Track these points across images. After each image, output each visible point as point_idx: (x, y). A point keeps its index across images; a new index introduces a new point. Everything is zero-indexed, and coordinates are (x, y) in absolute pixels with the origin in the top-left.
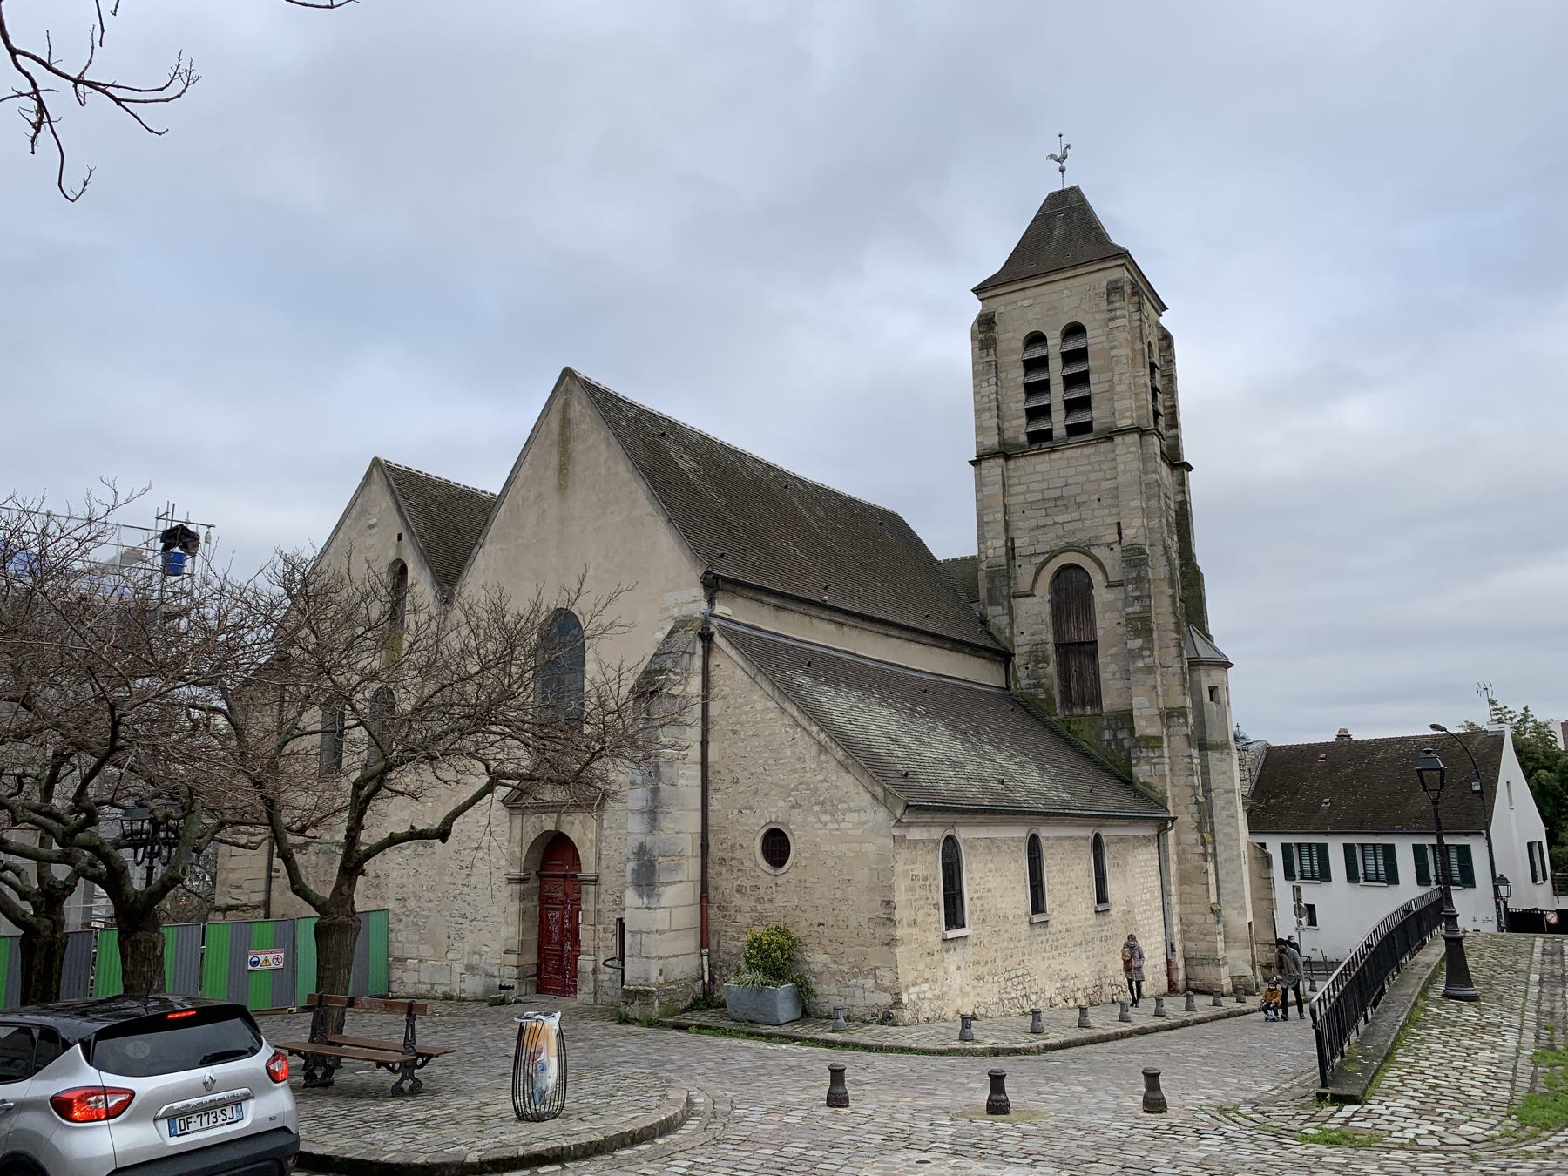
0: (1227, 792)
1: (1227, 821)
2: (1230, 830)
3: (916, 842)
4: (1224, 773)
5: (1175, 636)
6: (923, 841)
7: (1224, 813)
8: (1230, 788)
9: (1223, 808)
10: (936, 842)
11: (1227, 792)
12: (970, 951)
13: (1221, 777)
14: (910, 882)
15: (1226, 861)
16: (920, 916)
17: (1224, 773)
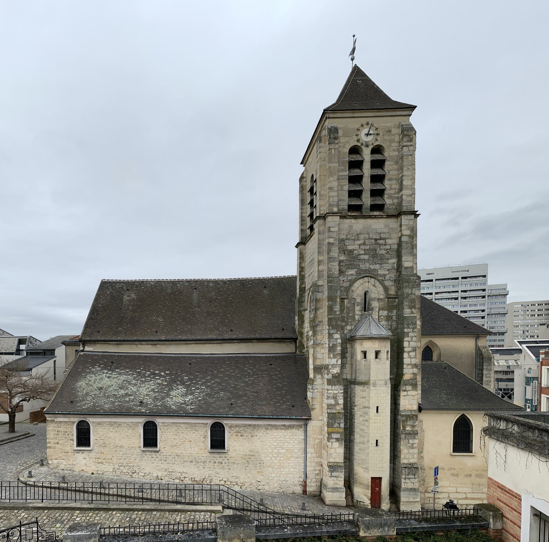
0: (364, 407)
1: (363, 423)
2: (364, 427)
3: (60, 422)
4: (364, 398)
5: (328, 328)
6: (66, 422)
7: (361, 419)
8: (367, 405)
9: (361, 416)
10: (74, 422)
11: (364, 407)
12: (93, 454)
13: (362, 399)
14: (56, 432)
15: (360, 443)
16: (61, 442)
17: (364, 398)
